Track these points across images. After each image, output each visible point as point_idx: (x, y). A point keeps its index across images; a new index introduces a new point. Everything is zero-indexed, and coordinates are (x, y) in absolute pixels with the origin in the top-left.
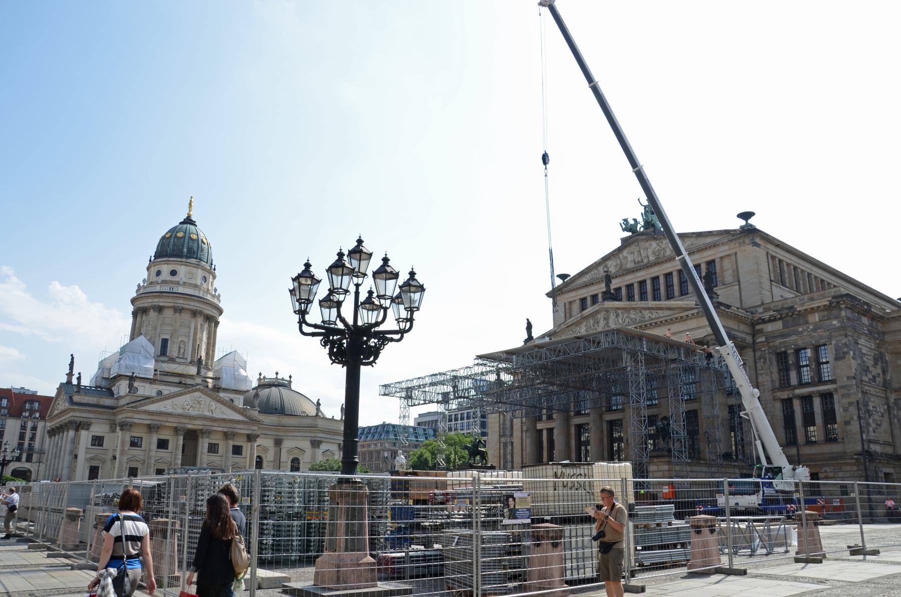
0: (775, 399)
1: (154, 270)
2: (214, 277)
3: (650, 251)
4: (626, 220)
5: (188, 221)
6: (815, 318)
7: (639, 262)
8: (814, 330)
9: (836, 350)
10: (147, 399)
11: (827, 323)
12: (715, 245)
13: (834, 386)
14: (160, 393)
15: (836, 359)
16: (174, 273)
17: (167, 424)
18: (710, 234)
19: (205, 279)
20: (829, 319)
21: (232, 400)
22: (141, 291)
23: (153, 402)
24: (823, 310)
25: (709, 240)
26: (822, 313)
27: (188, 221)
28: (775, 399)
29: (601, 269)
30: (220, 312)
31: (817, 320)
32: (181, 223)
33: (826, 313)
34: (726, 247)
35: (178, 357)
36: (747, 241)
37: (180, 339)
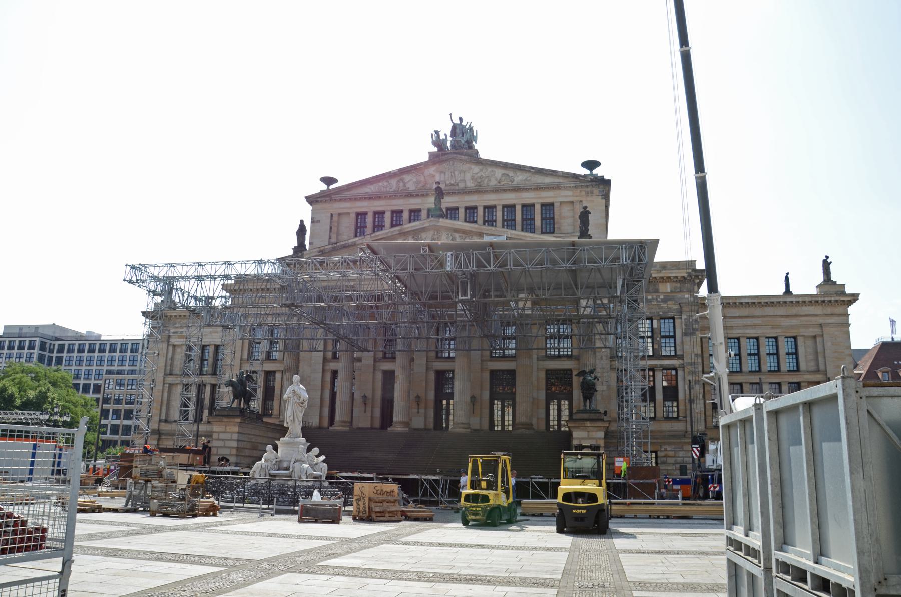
0: (612, 368)
3: (468, 176)
4: (437, 132)
6: (667, 288)
7: (452, 185)
8: (665, 300)
9: (686, 325)
11: (679, 295)
12: (558, 187)
13: (681, 361)
15: (685, 334)
18: (553, 173)
20: (681, 292)
24: (677, 282)
25: (548, 180)
26: (675, 285)
28: (612, 368)
29: (394, 182)
31: (669, 291)
33: (678, 285)
34: (570, 193)
36: (596, 191)
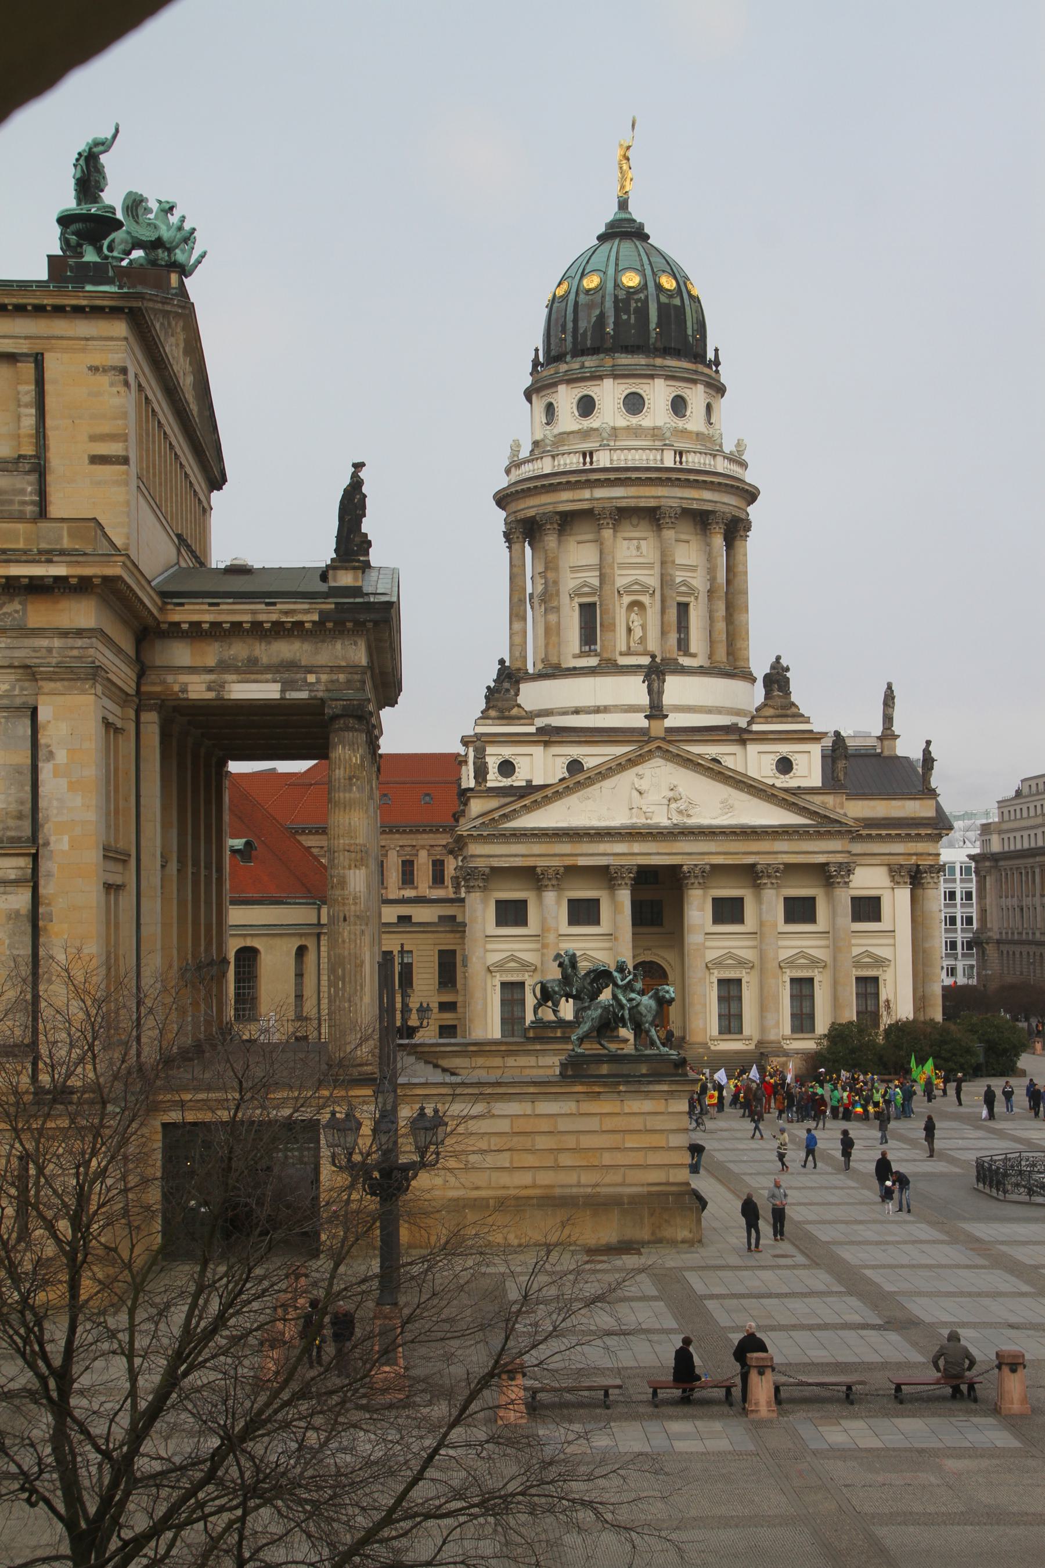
1: (539, 404)
2: (720, 390)
5: (625, 231)
10: (532, 795)
14: (575, 766)
16: (587, 406)
17: (582, 862)
19: (679, 405)
21: (785, 765)
22: (517, 475)
23: (536, 805)
27: (625, 231)
30: (751, 495)
32: (599, 238)
35: (628, 653)
37: (627, 599)
